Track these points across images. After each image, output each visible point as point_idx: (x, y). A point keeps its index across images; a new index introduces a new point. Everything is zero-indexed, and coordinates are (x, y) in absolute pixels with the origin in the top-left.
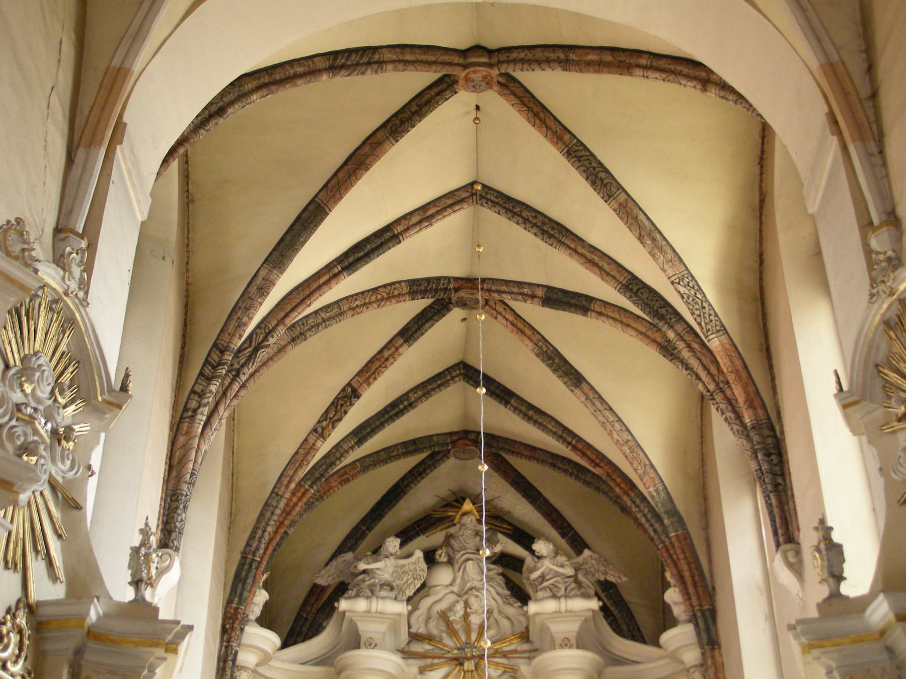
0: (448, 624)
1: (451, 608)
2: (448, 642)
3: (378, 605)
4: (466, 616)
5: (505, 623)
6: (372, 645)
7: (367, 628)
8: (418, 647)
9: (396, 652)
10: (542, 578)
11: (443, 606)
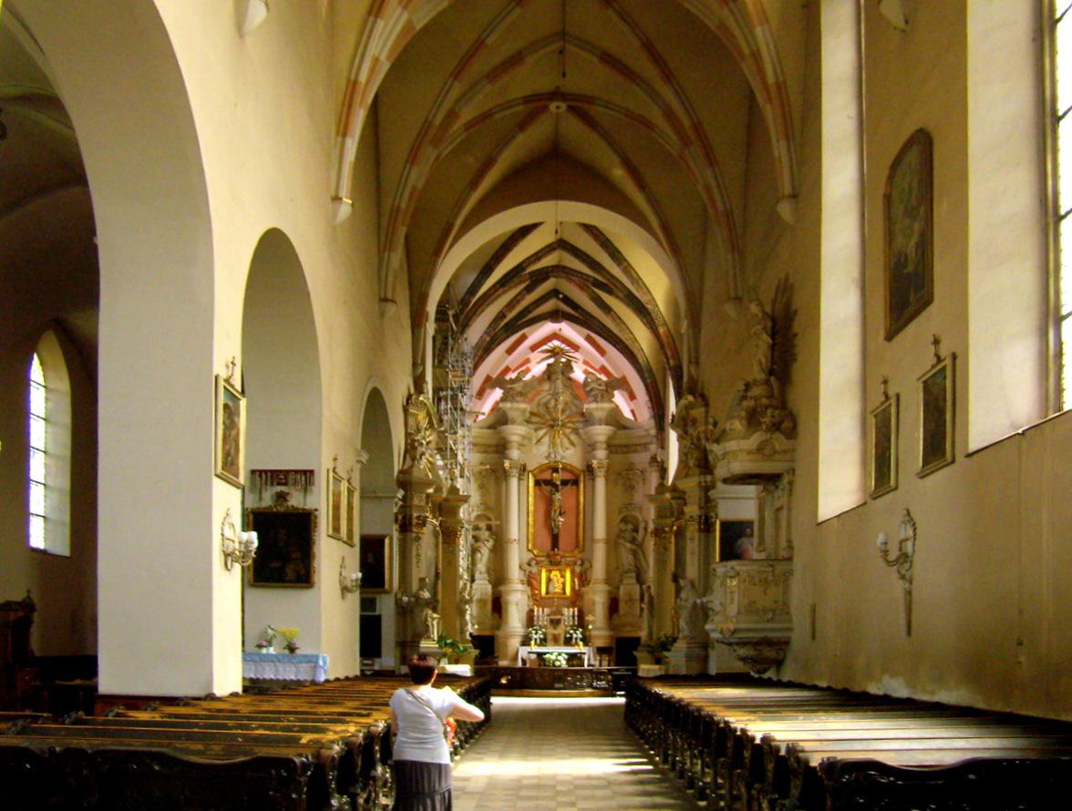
0: (547, 408)
1: (549, 401)
2: (548, 417)
3: (516, 405)
4: (556, 406)
5: (574, 408)
6: (513, 422)
7: (512, 414)
8: (535, 419)
9: (525, 423)
10: (592, 390)
11: (544, 400)
